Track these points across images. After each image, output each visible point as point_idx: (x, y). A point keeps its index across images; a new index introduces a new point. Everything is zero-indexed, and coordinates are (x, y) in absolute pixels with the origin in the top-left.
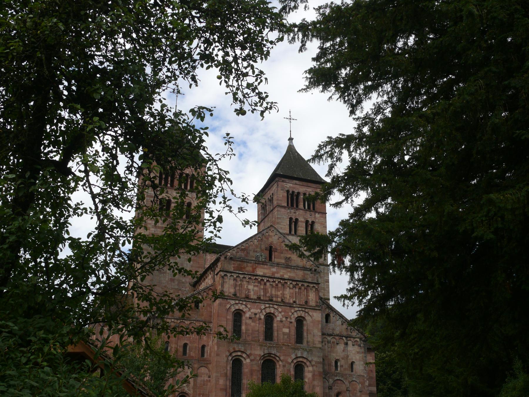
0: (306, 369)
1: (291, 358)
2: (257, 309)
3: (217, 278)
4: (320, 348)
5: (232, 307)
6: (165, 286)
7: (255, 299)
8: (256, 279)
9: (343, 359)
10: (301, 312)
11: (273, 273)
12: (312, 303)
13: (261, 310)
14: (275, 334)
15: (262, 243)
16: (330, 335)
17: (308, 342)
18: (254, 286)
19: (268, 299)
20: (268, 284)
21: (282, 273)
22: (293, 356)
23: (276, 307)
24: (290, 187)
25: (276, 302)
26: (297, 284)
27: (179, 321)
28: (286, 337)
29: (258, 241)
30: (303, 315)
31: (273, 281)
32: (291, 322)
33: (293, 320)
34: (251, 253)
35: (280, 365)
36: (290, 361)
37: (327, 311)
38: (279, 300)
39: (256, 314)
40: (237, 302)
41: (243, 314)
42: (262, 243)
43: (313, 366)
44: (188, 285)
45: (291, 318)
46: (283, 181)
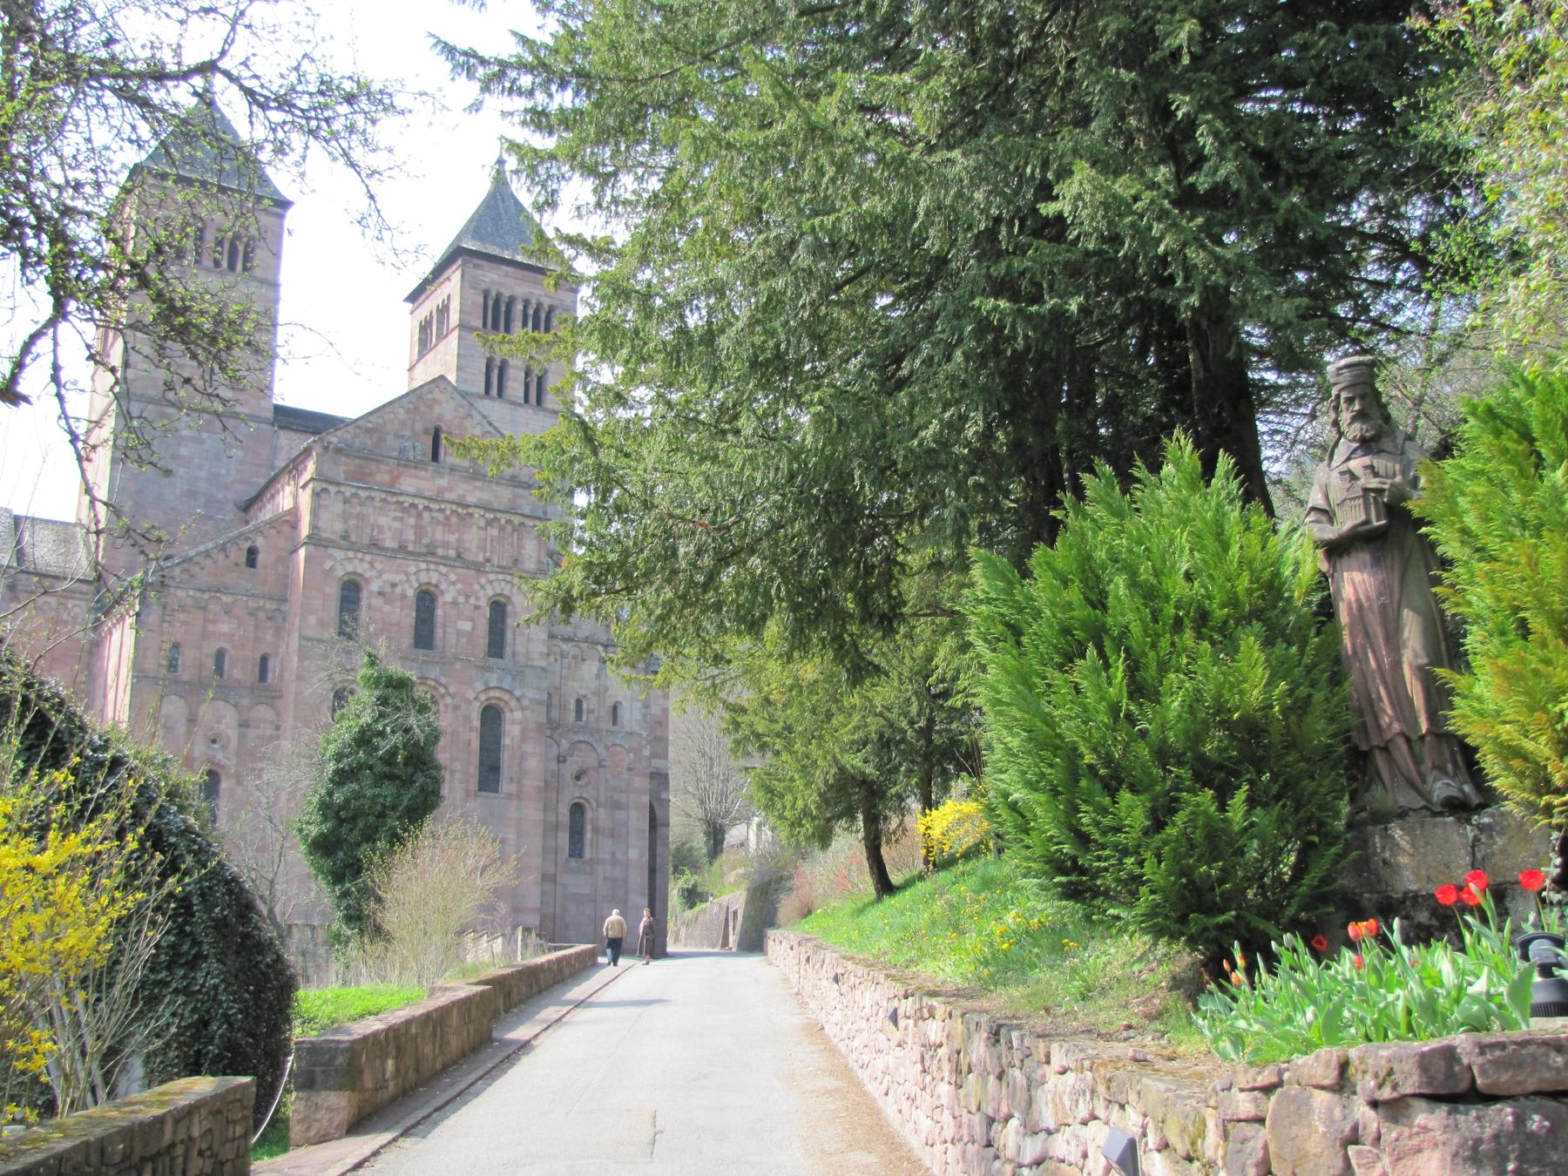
0: (508, 715)
2: (397, 572)
3: (305, 498)
4: (544, 669)
5: (339, 567)
6: (173, 509)
7: (393, 550)
8: (398, 502)
9: (594, 694)
11: (441, 491)
12: (530, 565)
13: (407, 574)
14: (439, 632)
16: (568, 640)
17: (514, 654)
18: (395, 519)
19: (424, 550)
20: (426, 515)
21: (460, 492)
22: (480, 686)
23: (443, 569)
24: (493, 282)
25: (443, 557)
26: (495, 519)
29: (409, 411)
30: (506, 592)
31: (441, 510)
32: (477, 607)
33: (483, 603)
34: (390, 441)
35: (446, 706)
36: (471, 695)
38: (452, 553)
39: (394, 585)
40: (351, 554)
41: (363, 583)
43: (523, 709)
44: (230, 506)
45: (477, 598)
46: (476, 266)
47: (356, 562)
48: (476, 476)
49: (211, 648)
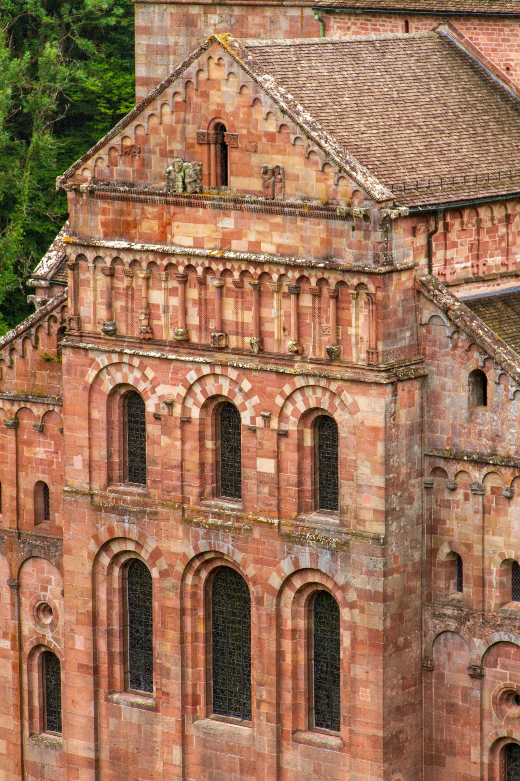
1: (279, 572)
4: (376, 539)
10: (319, 393)
15: (189, 117)
16: (480, 462)
21: (252, 237)
27: (16, 408)
28: (266, 490)
29: (177, 108)
32: (283, 434)
33: (292, 426)
36: (276, 582)
37: (476, 360)
42: (189, 117)
47: (125, 369)
48: (270, 208)
49: (28, 483)
